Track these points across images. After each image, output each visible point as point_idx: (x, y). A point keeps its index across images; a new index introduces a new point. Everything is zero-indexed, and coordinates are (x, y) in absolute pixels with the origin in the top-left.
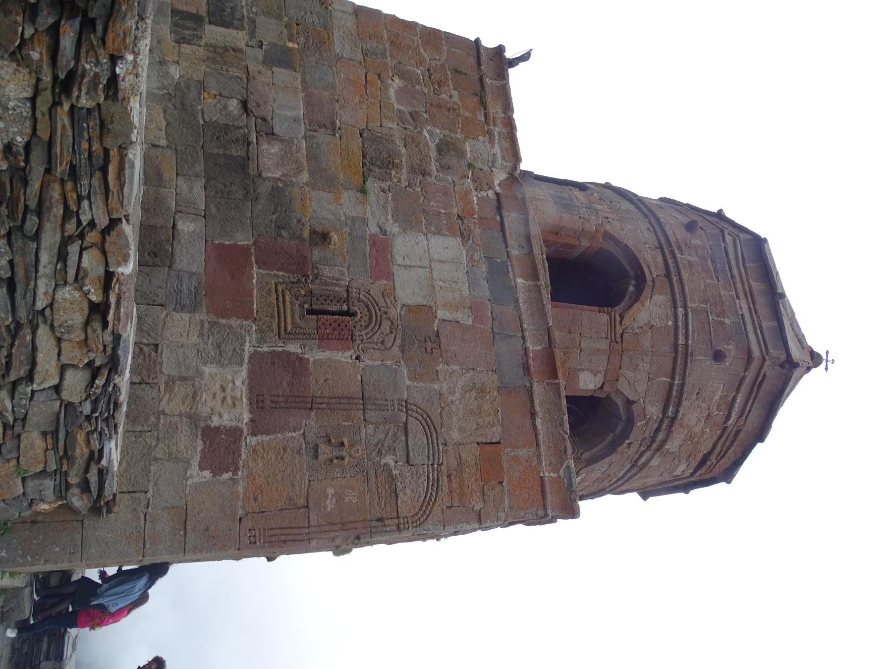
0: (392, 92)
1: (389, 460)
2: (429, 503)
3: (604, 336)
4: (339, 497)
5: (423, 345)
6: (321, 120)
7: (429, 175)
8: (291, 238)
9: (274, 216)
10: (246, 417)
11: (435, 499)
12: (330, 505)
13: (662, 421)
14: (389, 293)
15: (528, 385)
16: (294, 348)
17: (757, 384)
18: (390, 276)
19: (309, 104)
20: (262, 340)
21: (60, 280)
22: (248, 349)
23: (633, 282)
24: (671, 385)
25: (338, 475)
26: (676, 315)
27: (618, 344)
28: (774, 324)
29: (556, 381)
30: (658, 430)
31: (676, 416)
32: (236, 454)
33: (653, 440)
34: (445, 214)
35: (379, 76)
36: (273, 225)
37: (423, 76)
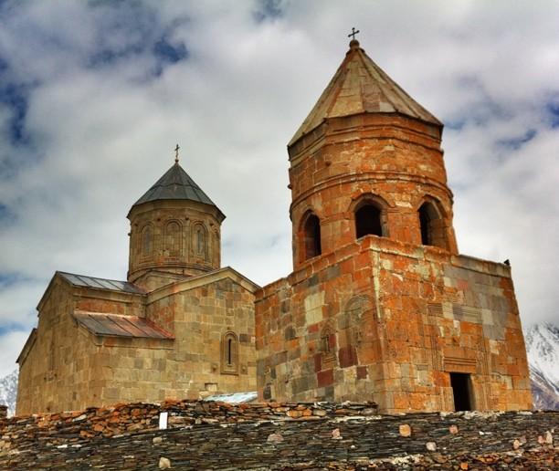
0: (274, 333)
1: (360, 315)
4: (370, 331)
6: (284, 357)
10: (354, 366)
12: (371, 334)
13: (360, 181)
14: (321, 323)
16: (337, 354)
18: (317, 325)
19: (282, 361)
20: (336, 365)
21: (285, 416)
22: (339, 369)
24: (343, 184)
32: (362, 368)
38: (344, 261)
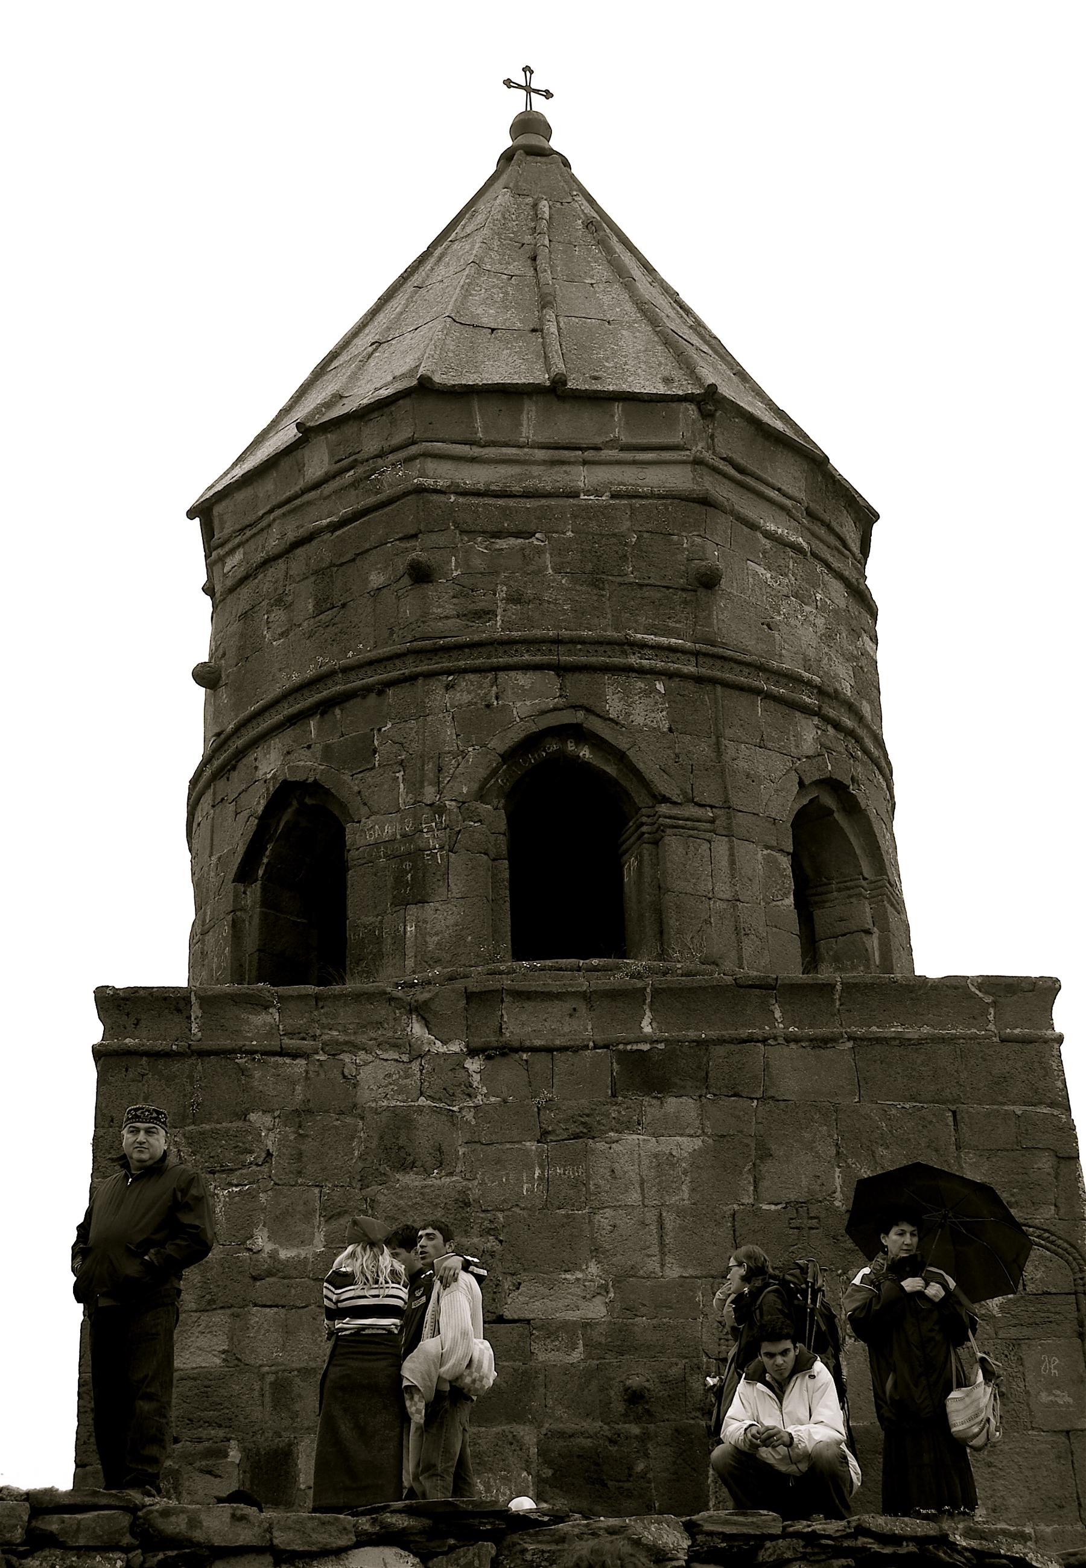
0: (284, 1254)
2: (1052, 1242)
3: (706, 845)
4: (1052, 1384)
5: (804, 1233)
7: (464, 1192)
8: (646, 1455)
9: (610, 1483)
11: (1046, 1231)
15: (850, 1044)
17: (742, 477)
23: (571, 747)
25: (1022, 1385)
26: (641, 672)
27: (723, 818)
28: (618, 409)
29: (839, 987)
30: (837, 726)
31: (816, 686)
33: (850, 733)
34: (542, 1167)
35: (255, 1279)
36: (626, 1485)
37: (231, 1185)
38: (903, 1042)
